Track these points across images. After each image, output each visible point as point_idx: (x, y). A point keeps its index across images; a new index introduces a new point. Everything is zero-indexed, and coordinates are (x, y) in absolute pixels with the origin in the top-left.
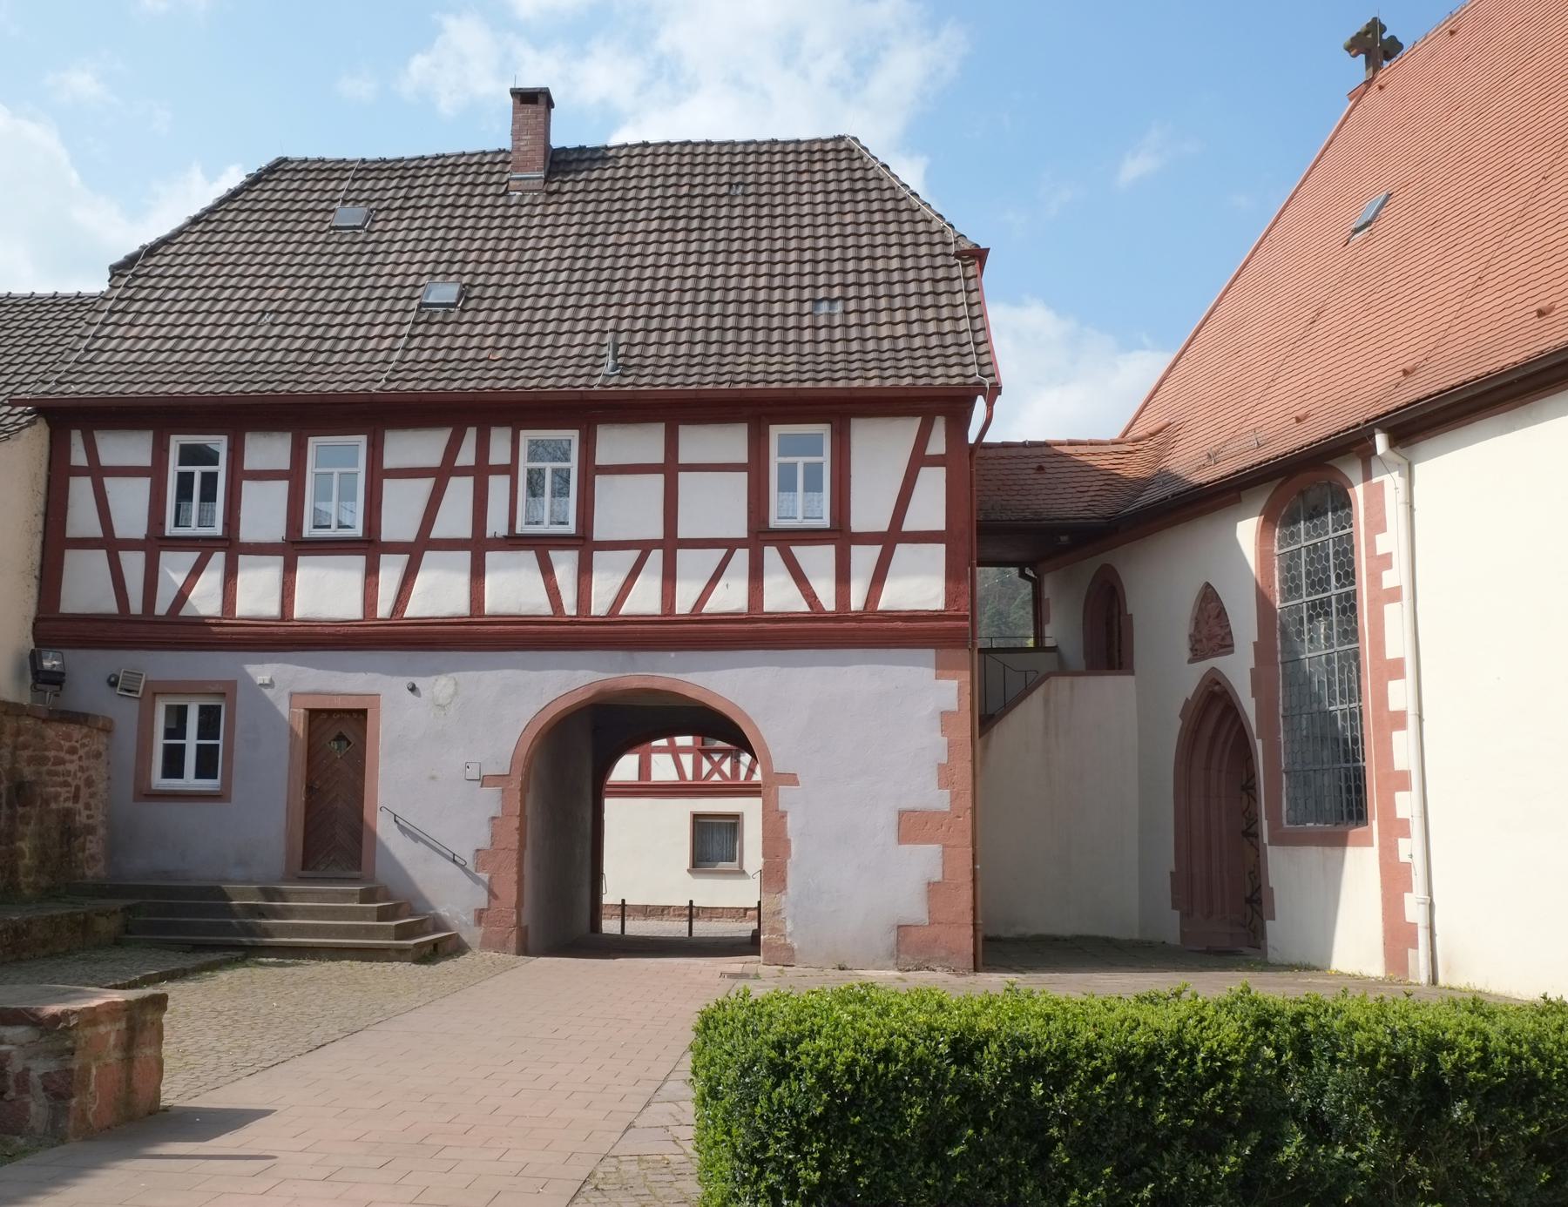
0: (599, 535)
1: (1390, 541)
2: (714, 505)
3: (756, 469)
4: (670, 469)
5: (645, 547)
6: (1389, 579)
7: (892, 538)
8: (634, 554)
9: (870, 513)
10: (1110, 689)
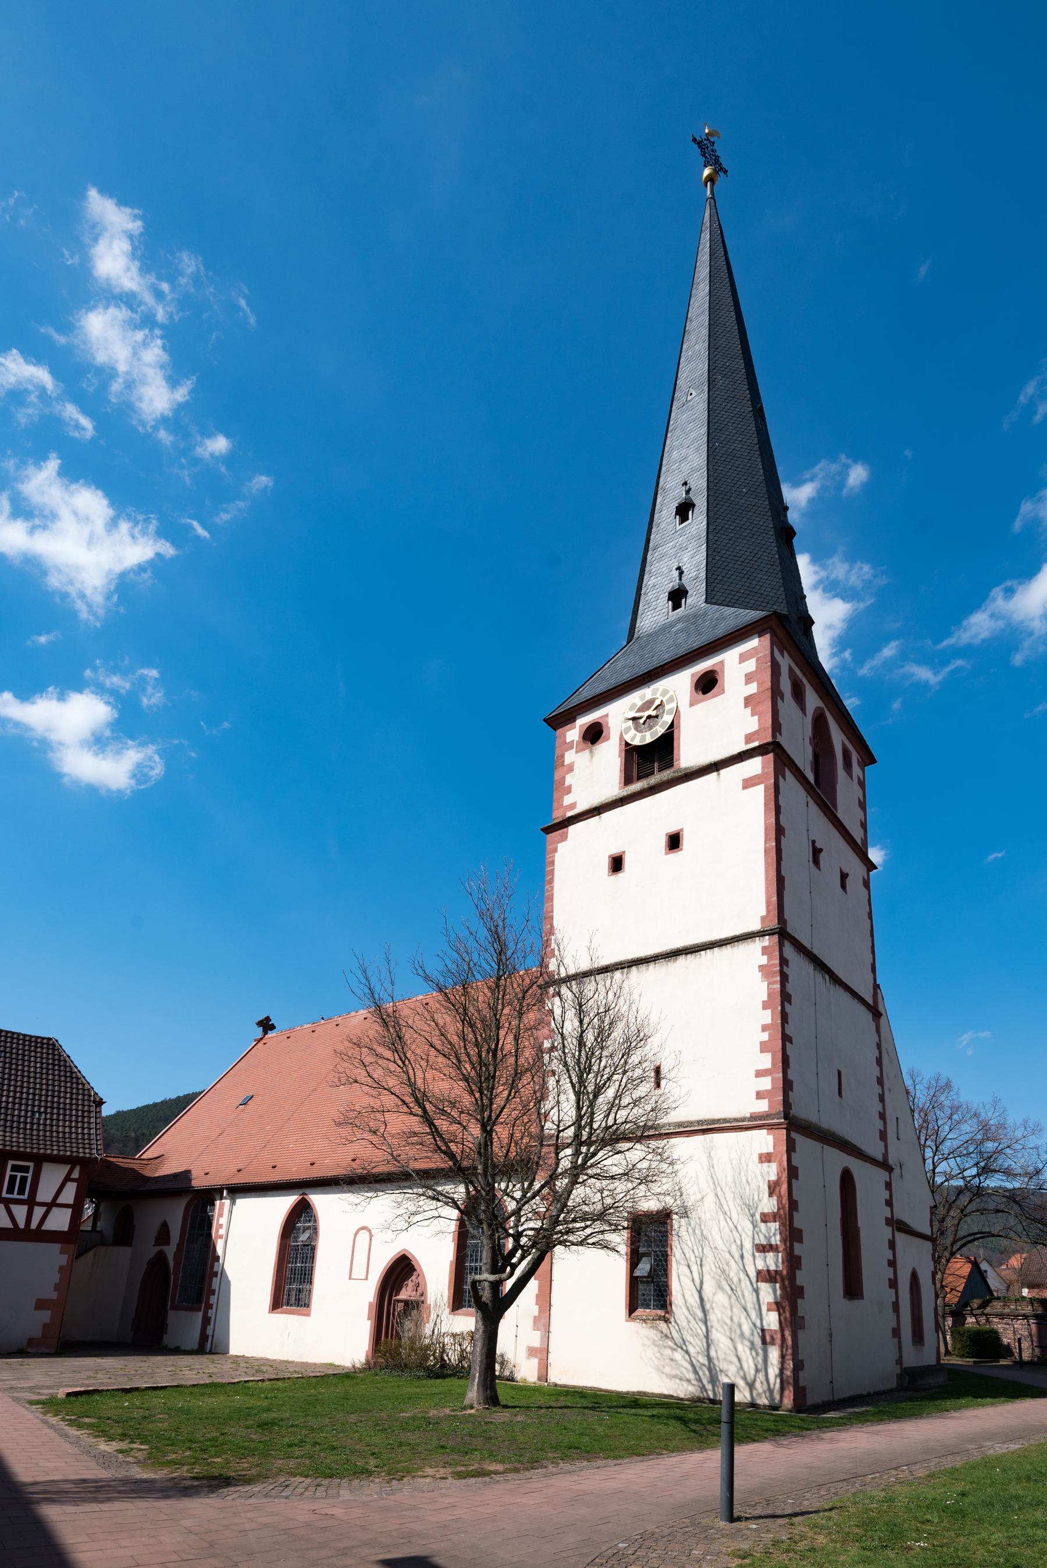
1: (223, 1221)
6: (222, 1232)
10: (124, 1252)
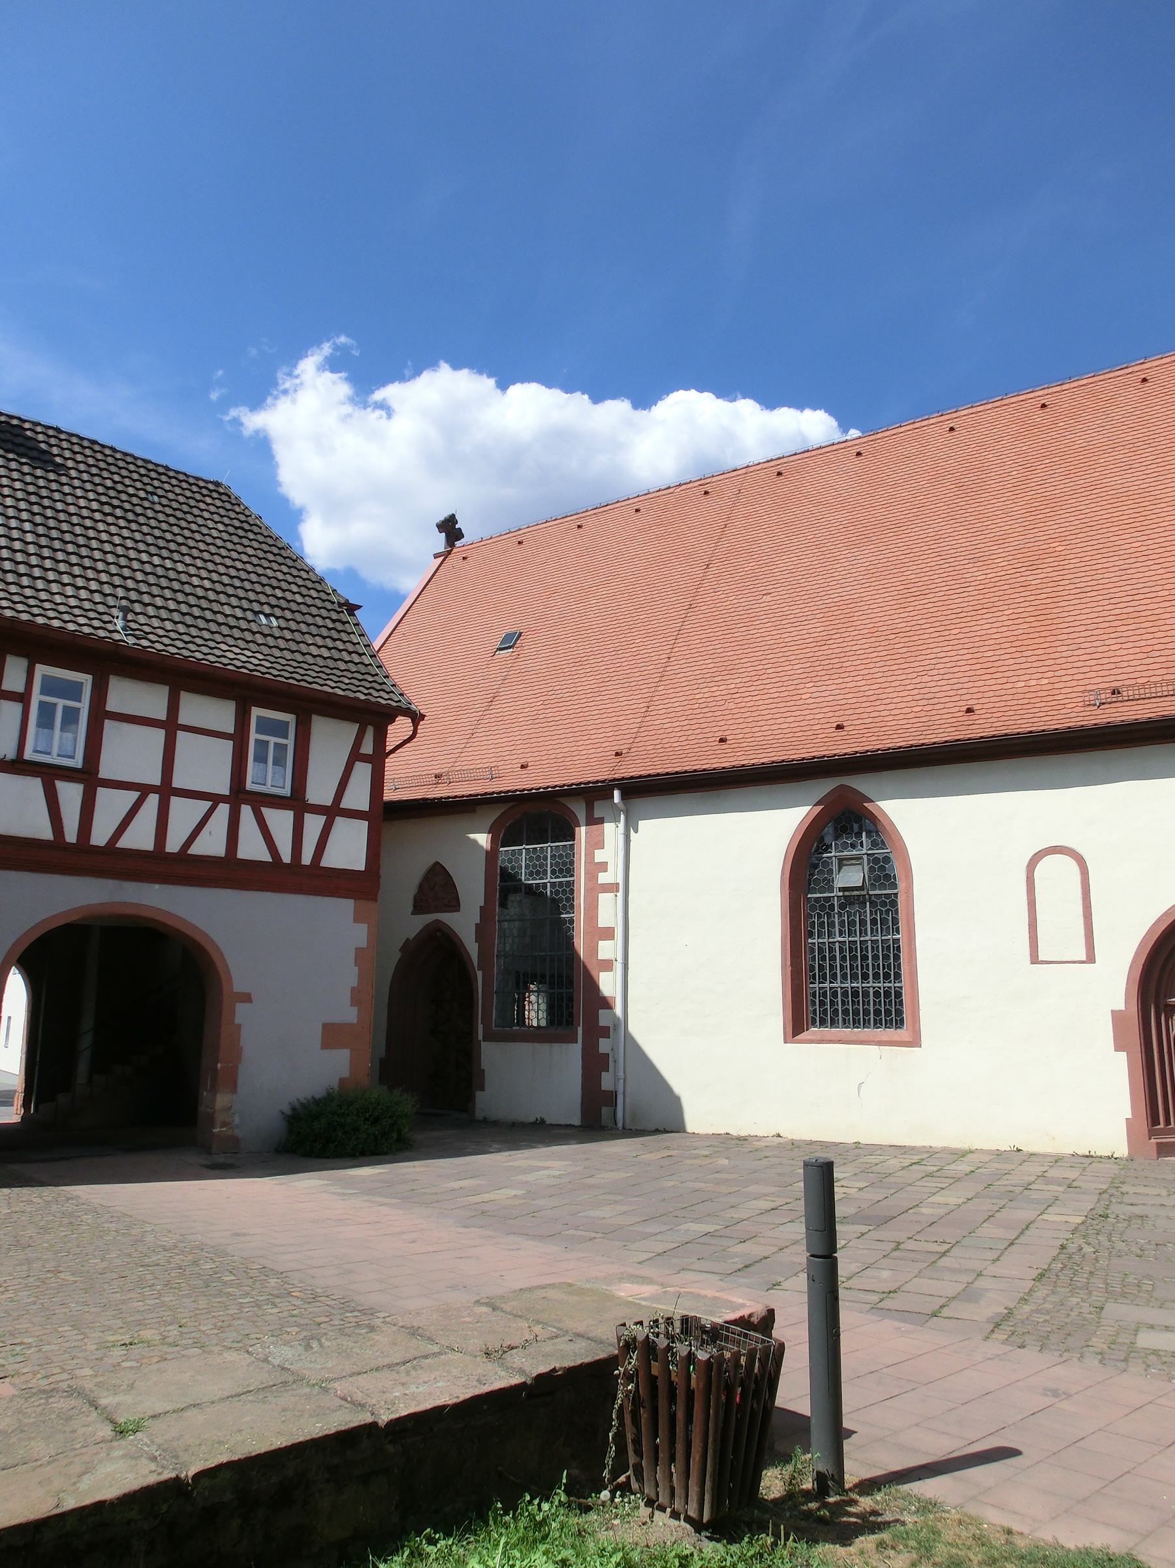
0: (104, 773)
2: (205, 765)
3: (239, 739)
4: (171, 726)
5: (144, 790)
7: (333, 812)
8: (134, 795)
9: (320, 791)
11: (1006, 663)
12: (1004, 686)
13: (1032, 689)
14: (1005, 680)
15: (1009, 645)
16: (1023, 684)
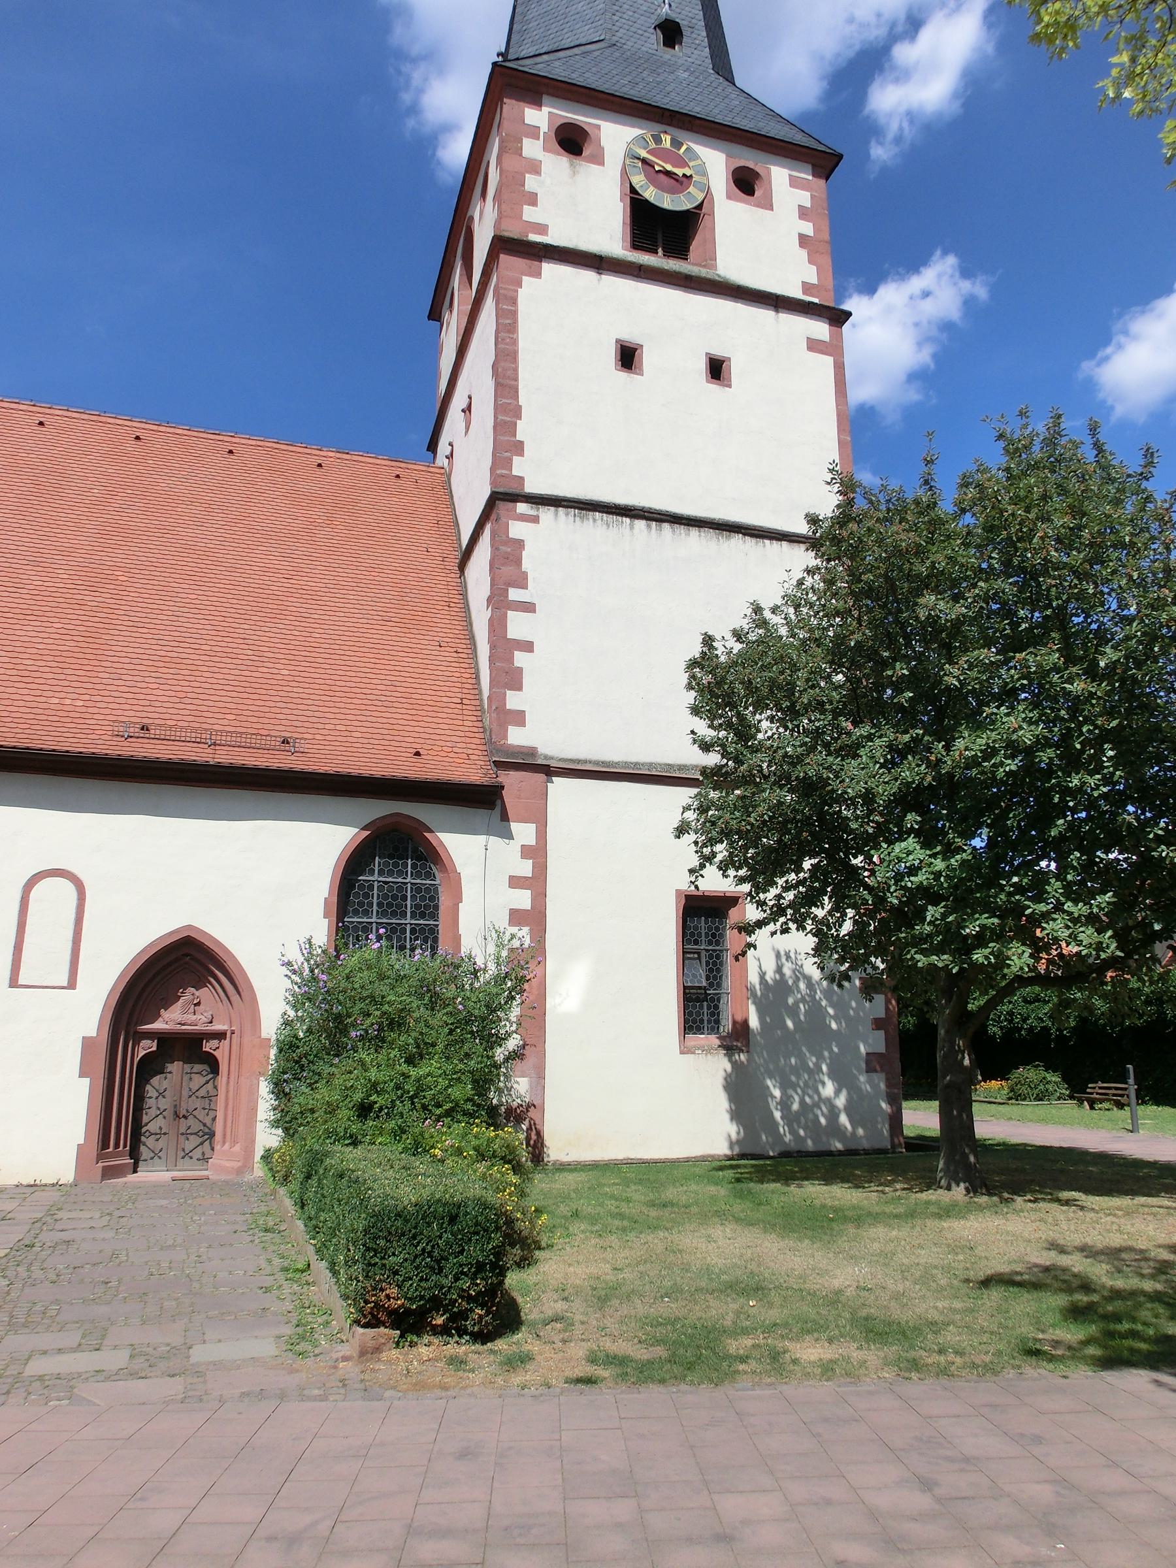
11: (44, 675)
12: (38, 699)
13: (65, 708)
14: (39, 693)
15: (51, 658)
16: (57, 701)
